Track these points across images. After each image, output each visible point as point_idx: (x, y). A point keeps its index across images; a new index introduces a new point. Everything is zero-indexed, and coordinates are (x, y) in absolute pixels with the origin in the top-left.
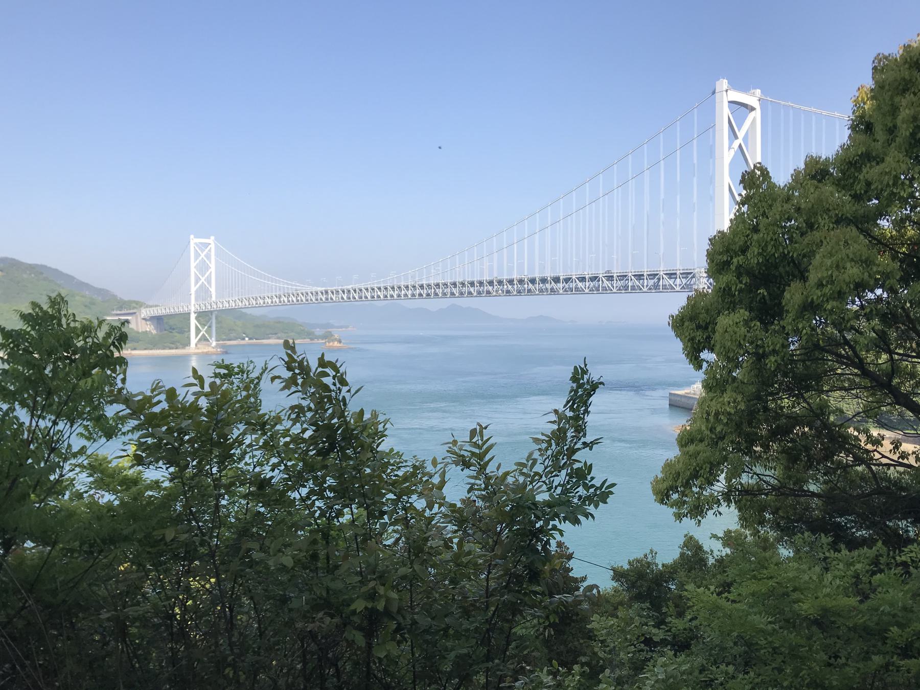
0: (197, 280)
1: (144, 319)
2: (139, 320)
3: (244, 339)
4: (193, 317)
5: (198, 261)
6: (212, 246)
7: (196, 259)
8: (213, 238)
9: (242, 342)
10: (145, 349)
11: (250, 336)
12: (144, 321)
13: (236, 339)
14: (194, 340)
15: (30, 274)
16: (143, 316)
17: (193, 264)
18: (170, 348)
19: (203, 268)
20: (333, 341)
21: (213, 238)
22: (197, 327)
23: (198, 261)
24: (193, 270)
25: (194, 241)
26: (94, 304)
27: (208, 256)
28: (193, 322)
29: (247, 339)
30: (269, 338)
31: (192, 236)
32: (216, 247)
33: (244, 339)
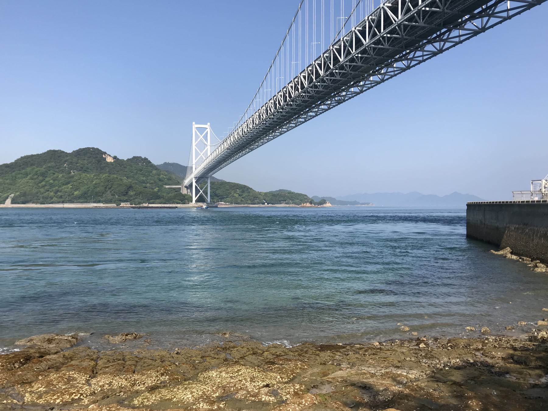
0: (197, 154)
1: (185, 187)
2: (184, 187)
3: (264, 204)
4: (194, 181)
5: (197, 142)
6: (208, 130)
7: (196, 140)
8: (209, 124)
9: (261, 205)
10: (160, 203)
11: (268, 202)
12: (186, 189)
13: (258, 203)
14: (194, 199)
15: (143, 163)
16: (185, 184)
17: (194, 144)
18: (177, 203)
19: (201, 146)
20: (306, 202)
21: (209, 124)
22: (196, 187)
23: (197, 142)
24: (194, 147)
25: (195, 126)
26: (170, 180)
27: (206, 137)
28: (194, 184)
29: (266, 204)
30: (281, 203)
31: (194, 123)
32: (211, 131)
33: (264, 204)
